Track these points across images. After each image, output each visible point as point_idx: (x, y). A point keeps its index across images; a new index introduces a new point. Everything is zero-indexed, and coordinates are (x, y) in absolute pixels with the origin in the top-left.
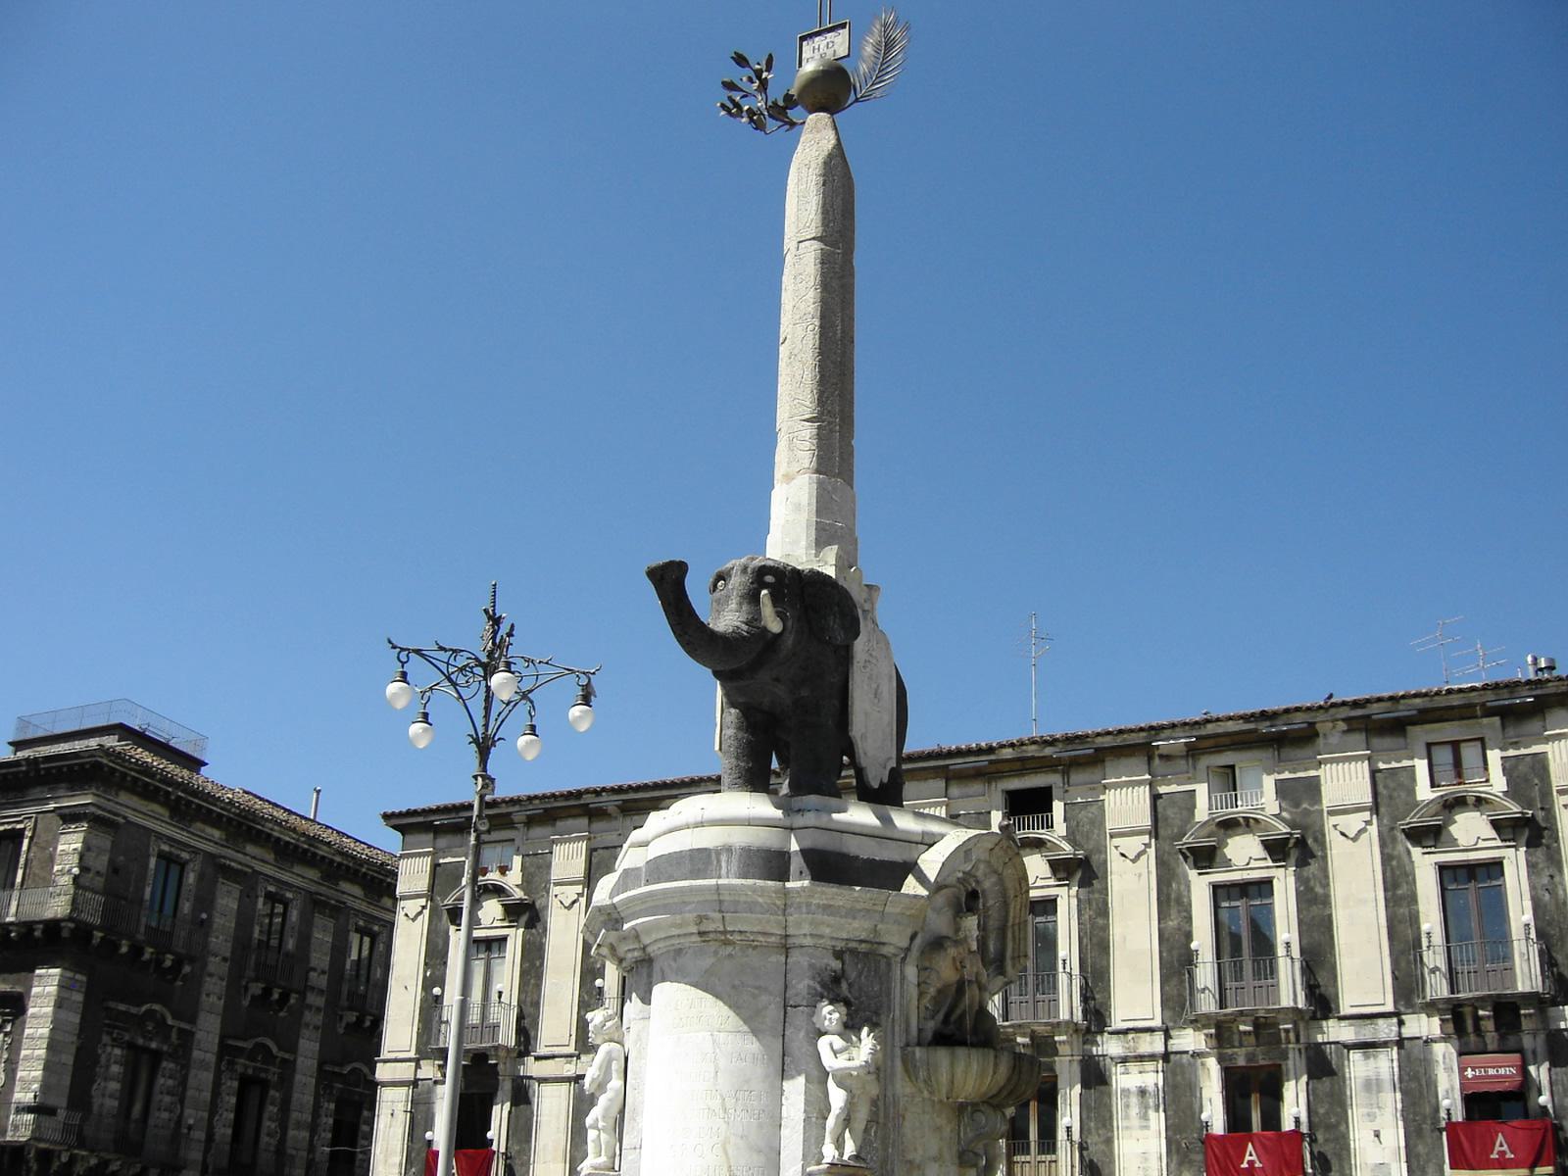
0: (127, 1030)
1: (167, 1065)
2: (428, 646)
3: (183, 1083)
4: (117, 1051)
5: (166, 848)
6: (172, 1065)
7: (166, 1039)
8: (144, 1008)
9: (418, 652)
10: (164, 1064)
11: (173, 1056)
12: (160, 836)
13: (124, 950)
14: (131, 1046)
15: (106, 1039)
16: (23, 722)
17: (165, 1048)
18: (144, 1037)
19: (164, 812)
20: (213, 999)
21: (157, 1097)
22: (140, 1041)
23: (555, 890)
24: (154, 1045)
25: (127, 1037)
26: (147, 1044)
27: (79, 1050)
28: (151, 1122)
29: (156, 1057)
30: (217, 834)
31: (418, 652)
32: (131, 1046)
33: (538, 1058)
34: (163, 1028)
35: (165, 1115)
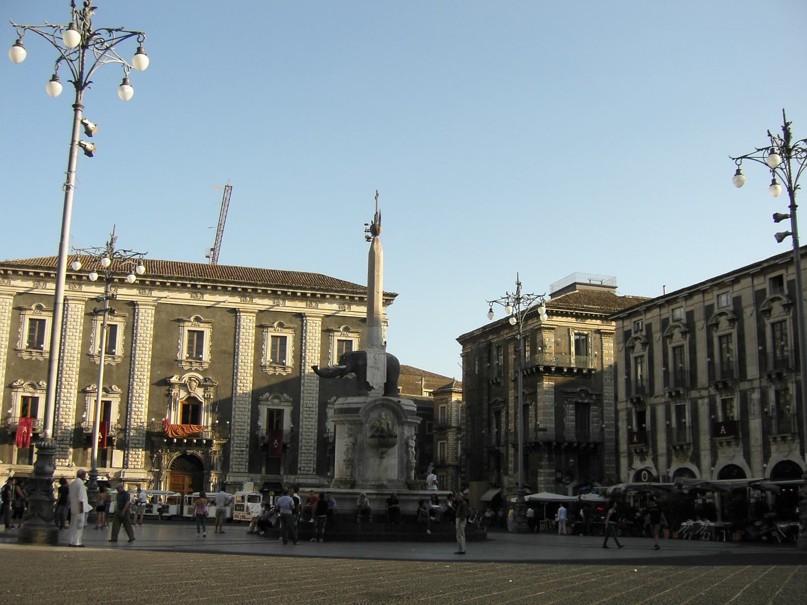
0: (573, 398)
1: (593, 407)
2: (497, 298)
3: (602, 412)
4: (571, 406)
5: (576, 331)
6: (595, 407)
7: (591, 399)
8: (578, 390)
9: (495, 301)
10: (592, 407)
11: (594, 404)
12: (574, 328)
13: (565, 370)
14: (577, 404)
15: (565, 402)
16: (552, 286)
17: (591, 401)
18: (581, 399)
19: (574, 320)
20: (608, 381)
21: (591, 419)
22: (580, 401)
23: (654, 336)
24: (586, 401)
25: (574, 400)
26: (583, 401)
27: (555, 408)
28: (591, 428)
29: (588, 405)
30: (599, 322)
31: (495, 301)
32: (577, 404)
33: (655, 397)
34: (589, 395)
35: (596, 425)
